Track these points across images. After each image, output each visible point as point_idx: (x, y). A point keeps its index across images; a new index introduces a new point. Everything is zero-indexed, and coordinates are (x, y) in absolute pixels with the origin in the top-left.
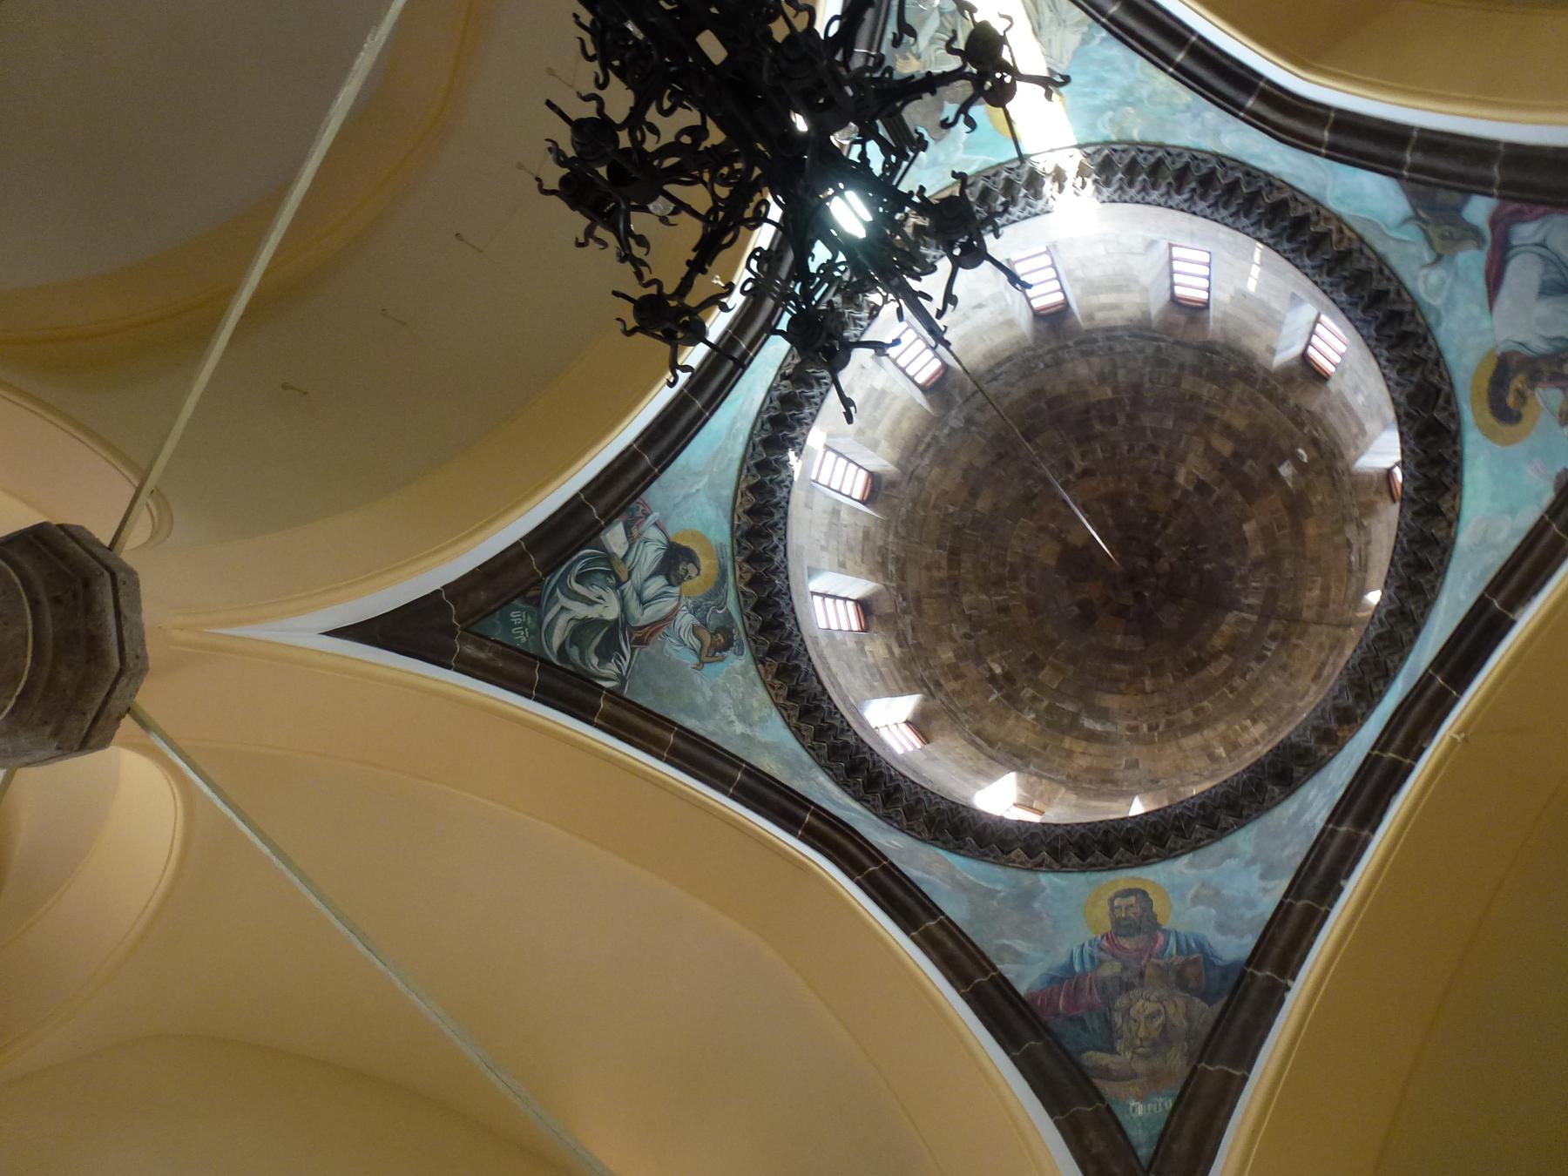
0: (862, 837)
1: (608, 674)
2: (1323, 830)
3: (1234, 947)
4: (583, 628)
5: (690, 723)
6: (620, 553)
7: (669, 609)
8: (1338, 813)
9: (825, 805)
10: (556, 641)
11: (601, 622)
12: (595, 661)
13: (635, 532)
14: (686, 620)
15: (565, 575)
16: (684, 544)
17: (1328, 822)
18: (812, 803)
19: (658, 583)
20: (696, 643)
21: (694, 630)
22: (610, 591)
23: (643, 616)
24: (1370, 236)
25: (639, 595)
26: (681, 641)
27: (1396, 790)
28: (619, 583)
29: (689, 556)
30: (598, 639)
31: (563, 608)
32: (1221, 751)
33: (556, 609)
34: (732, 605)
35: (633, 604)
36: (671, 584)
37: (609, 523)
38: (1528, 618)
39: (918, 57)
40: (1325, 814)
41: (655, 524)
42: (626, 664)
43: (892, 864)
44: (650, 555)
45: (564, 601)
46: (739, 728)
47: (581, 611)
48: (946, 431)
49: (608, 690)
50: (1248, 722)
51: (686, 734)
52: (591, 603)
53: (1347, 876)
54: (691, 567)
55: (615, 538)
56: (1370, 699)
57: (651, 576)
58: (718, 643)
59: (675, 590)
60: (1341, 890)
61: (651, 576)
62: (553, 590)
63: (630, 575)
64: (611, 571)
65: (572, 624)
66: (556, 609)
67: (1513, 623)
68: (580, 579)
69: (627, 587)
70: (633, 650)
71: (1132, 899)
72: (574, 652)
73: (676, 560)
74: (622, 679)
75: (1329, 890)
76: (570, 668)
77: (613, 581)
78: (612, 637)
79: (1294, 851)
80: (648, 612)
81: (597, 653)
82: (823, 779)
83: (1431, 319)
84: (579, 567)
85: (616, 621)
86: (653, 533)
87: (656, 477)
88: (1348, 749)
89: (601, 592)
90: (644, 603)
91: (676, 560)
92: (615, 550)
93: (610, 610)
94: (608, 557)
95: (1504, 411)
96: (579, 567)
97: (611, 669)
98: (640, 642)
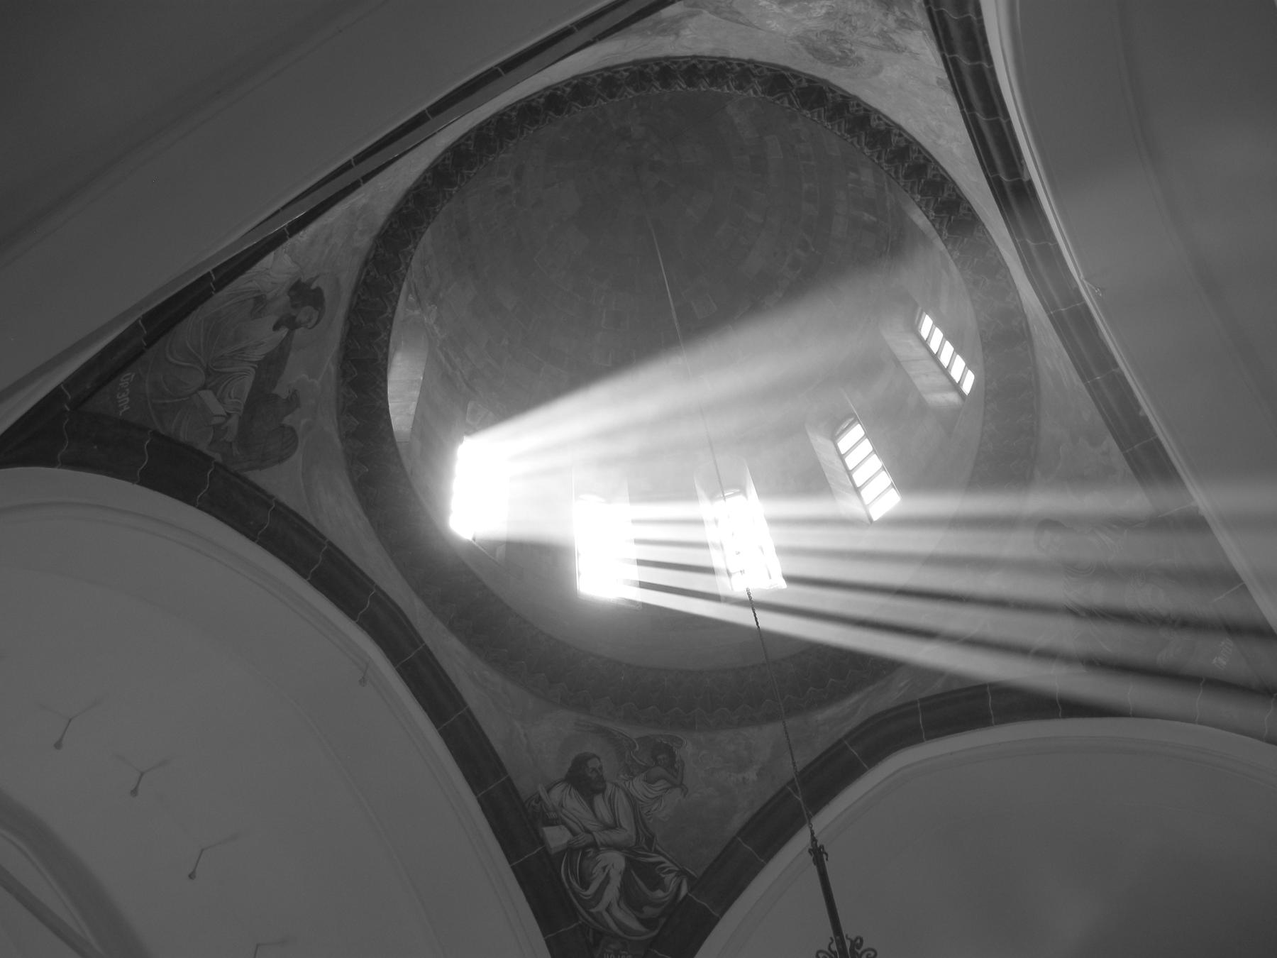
0: (888, 711)
1: (673, 885)
4: (628, 895)
5: (737, 822)
6: (568, 835)
7: (625, 800)
9: (847, 729)
10: (634, 925)
11: (626, 875)
12: (659, 894)
13: (553, 815)
14: (638, 786)
15: (574, 893)
16: (569, 765)
17: (1083, 379)
18: (840, 741)
19: (599, 802)
20: (661, 784)
21: (650, 781)
22: (600, 857)
23: (627, 832)
25: (608, 827)
26: (658, 798)
28: (594, 845)
29: (581, 761)
30: (640, 883)
31: (608, 910)
32: (867, 217)
33: (605, 914)
34: (634, 733)
35: (616, 837)
36: (603, 791)
37: (542, 841)
39: (229, 415)
40: (1075, 377)
41: (549, 790)
42: (668, 864)
43: (922, 700)
44: (573, 804)
45: (601, 907)
46: (751, 775)
47: (612, 893)
48: (437, 330)
49: (691, 889)
50: (853, 175)
51: (748, 831)
52: (607, 880)
53: (1139, 407)
54: (592, 764)
55: (556, 838)
57: (593, 811)
58: (664, 762)
59: (609, 786)
61: (593, 811)
62: (590, 914)
63: (588, 832)
64: (581, 852)
65: (622, 905)
66: (605, 914)
67: (1030, 183)
68: (585, 884)
69: (600, 837)
70: (657, 852)
72: (649, 911)
73: (582, 779)
74: (682, 873)
75: (1143, 426)
76: (663, 920)
77: (591, 851)
78: (641, 871)
79: (1088, 412)
80: (624, 823)
81: (653, 889)
82: (821, 716)
83: (718, 54)
84: (574, 883)
85: (627, 859)
86: (556, 794)
87: (509, 779)
88: (1035, 330)
89: (600, 865)
90: (615, 826)
91: (582, 779)
92: (565, 841)
93: (616, 862)
94: (570, 850)
95: (844, 59)
96: (574, 883)
97: (670, 880)
98: (650, 840)
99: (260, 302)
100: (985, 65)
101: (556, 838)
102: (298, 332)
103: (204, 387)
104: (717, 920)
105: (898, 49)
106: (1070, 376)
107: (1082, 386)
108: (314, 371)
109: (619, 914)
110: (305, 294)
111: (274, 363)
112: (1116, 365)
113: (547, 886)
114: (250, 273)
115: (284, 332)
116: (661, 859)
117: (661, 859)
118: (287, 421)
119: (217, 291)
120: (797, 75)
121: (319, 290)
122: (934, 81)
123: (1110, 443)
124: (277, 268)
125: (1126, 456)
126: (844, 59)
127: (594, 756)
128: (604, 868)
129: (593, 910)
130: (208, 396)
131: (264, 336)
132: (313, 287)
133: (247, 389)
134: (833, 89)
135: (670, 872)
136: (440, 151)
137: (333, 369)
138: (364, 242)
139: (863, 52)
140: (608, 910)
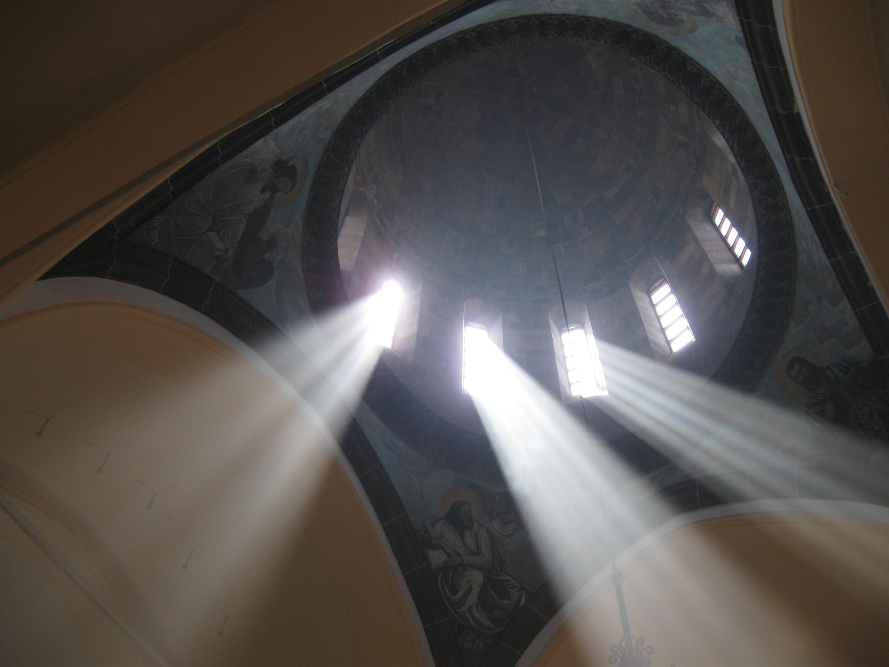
2: (832, 264)
3: (862, 351)
8: (829, 252)
10: (487, 622)
12: (506, 602)
17: (829, 258)
19: (468, 535)
24: (504, 17)
27: (840, 222)
30: (493, 593)
31: (469, 610)
32: (681, 137)
33: (468, 615)
38: (802, 106)
39: (227, 250)
40: (823, 256)
41: (433, 525)
42: (513, 582)
47: (472, 599)
48: (375, 201)
52: (470, 590)
53: (868, 280)
55: (436, 558)
56: (777, 190)
60: (872, 288)
63: (459, 555)
66: (468, 615)
67: (799, 115)
68: (455, 593)
71: (797, 366)
75: (870, 293)
83: (581, 14)
88: (796, 221)
90: (478, 552)
93: (478, 577)
95: (671, 21)
99: (252, 173)
100: (771, 28)
101: (436, 558)
102: (278, 195)
103: (211, 230)
104: (545, 624)
105: (709, 14)
106: (820, 256)
107: (827, 262)
108: (287, 223)
109: (477, 615)
110: (283, 169)
111: (260, 216)
112: (852, 248)
113: (430, 592)
114: (245, 152)
115: (267, 195)
116: (509, 578)
117: (509, 578)
118: (267, 256)
119: (223, 163)
120: (636, 31)
121: (293, 167)
122: (733, 38)
123: (845, 303)
124: (265, 149)
125: (856, 314)
126: (671, 21)
127: (467, 503)
128: (468, 581)
129: (459, 610)
130: (213, 236)
131: (255, 195)
132: (290, 164)
133: (241, 232)
134: (661, 42)
135: (514, 587)
136: (382, 74)
137: (301, 223)
138: (326, 135)
139: (684, 16)
140: (469, 610)
